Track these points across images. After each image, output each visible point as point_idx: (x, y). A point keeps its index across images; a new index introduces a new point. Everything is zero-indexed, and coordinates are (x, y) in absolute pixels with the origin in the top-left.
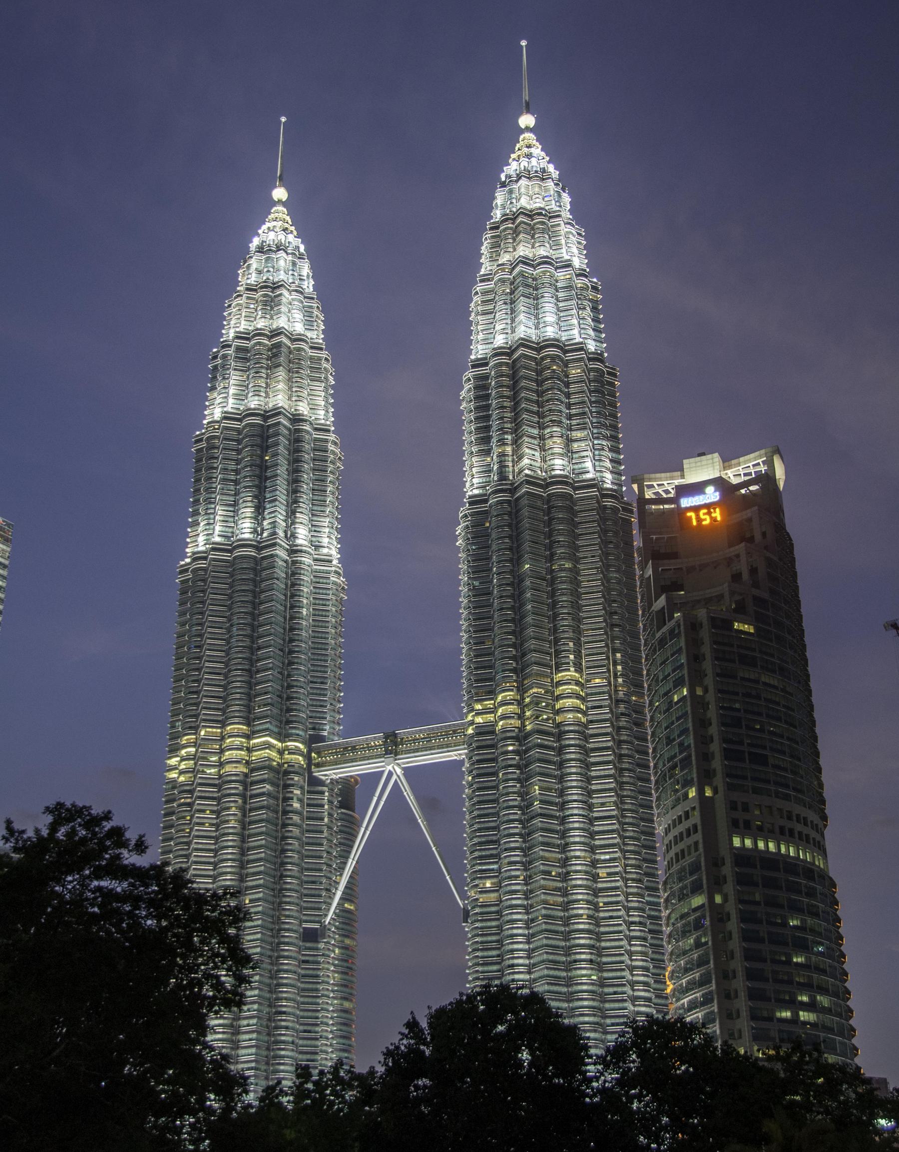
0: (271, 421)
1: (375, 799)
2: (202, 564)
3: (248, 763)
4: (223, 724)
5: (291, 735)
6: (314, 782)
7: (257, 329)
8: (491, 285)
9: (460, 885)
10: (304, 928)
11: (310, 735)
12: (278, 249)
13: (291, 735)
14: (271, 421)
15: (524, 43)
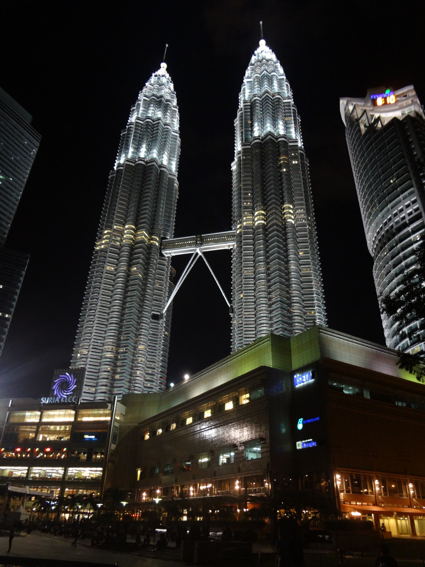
0: (155, 123)
1: (190, 262)
2: (121, 168)
3: (134, 241)
4: (124, 225)
5: (154, 233)
6: (162, 255)
7: (148, 116)
8: (251, 80)
9: (229, 297)
10: (153, 313)
11: (162, 237)
12: (163, 76)
13: (154, 233)
14: (155, 123)
15: (261, 23)
